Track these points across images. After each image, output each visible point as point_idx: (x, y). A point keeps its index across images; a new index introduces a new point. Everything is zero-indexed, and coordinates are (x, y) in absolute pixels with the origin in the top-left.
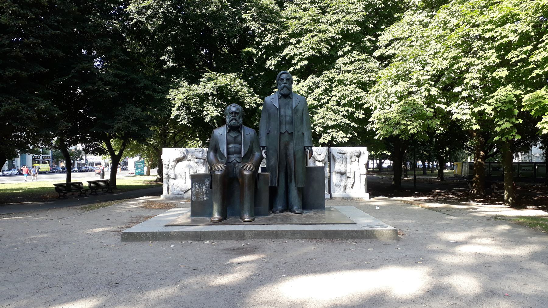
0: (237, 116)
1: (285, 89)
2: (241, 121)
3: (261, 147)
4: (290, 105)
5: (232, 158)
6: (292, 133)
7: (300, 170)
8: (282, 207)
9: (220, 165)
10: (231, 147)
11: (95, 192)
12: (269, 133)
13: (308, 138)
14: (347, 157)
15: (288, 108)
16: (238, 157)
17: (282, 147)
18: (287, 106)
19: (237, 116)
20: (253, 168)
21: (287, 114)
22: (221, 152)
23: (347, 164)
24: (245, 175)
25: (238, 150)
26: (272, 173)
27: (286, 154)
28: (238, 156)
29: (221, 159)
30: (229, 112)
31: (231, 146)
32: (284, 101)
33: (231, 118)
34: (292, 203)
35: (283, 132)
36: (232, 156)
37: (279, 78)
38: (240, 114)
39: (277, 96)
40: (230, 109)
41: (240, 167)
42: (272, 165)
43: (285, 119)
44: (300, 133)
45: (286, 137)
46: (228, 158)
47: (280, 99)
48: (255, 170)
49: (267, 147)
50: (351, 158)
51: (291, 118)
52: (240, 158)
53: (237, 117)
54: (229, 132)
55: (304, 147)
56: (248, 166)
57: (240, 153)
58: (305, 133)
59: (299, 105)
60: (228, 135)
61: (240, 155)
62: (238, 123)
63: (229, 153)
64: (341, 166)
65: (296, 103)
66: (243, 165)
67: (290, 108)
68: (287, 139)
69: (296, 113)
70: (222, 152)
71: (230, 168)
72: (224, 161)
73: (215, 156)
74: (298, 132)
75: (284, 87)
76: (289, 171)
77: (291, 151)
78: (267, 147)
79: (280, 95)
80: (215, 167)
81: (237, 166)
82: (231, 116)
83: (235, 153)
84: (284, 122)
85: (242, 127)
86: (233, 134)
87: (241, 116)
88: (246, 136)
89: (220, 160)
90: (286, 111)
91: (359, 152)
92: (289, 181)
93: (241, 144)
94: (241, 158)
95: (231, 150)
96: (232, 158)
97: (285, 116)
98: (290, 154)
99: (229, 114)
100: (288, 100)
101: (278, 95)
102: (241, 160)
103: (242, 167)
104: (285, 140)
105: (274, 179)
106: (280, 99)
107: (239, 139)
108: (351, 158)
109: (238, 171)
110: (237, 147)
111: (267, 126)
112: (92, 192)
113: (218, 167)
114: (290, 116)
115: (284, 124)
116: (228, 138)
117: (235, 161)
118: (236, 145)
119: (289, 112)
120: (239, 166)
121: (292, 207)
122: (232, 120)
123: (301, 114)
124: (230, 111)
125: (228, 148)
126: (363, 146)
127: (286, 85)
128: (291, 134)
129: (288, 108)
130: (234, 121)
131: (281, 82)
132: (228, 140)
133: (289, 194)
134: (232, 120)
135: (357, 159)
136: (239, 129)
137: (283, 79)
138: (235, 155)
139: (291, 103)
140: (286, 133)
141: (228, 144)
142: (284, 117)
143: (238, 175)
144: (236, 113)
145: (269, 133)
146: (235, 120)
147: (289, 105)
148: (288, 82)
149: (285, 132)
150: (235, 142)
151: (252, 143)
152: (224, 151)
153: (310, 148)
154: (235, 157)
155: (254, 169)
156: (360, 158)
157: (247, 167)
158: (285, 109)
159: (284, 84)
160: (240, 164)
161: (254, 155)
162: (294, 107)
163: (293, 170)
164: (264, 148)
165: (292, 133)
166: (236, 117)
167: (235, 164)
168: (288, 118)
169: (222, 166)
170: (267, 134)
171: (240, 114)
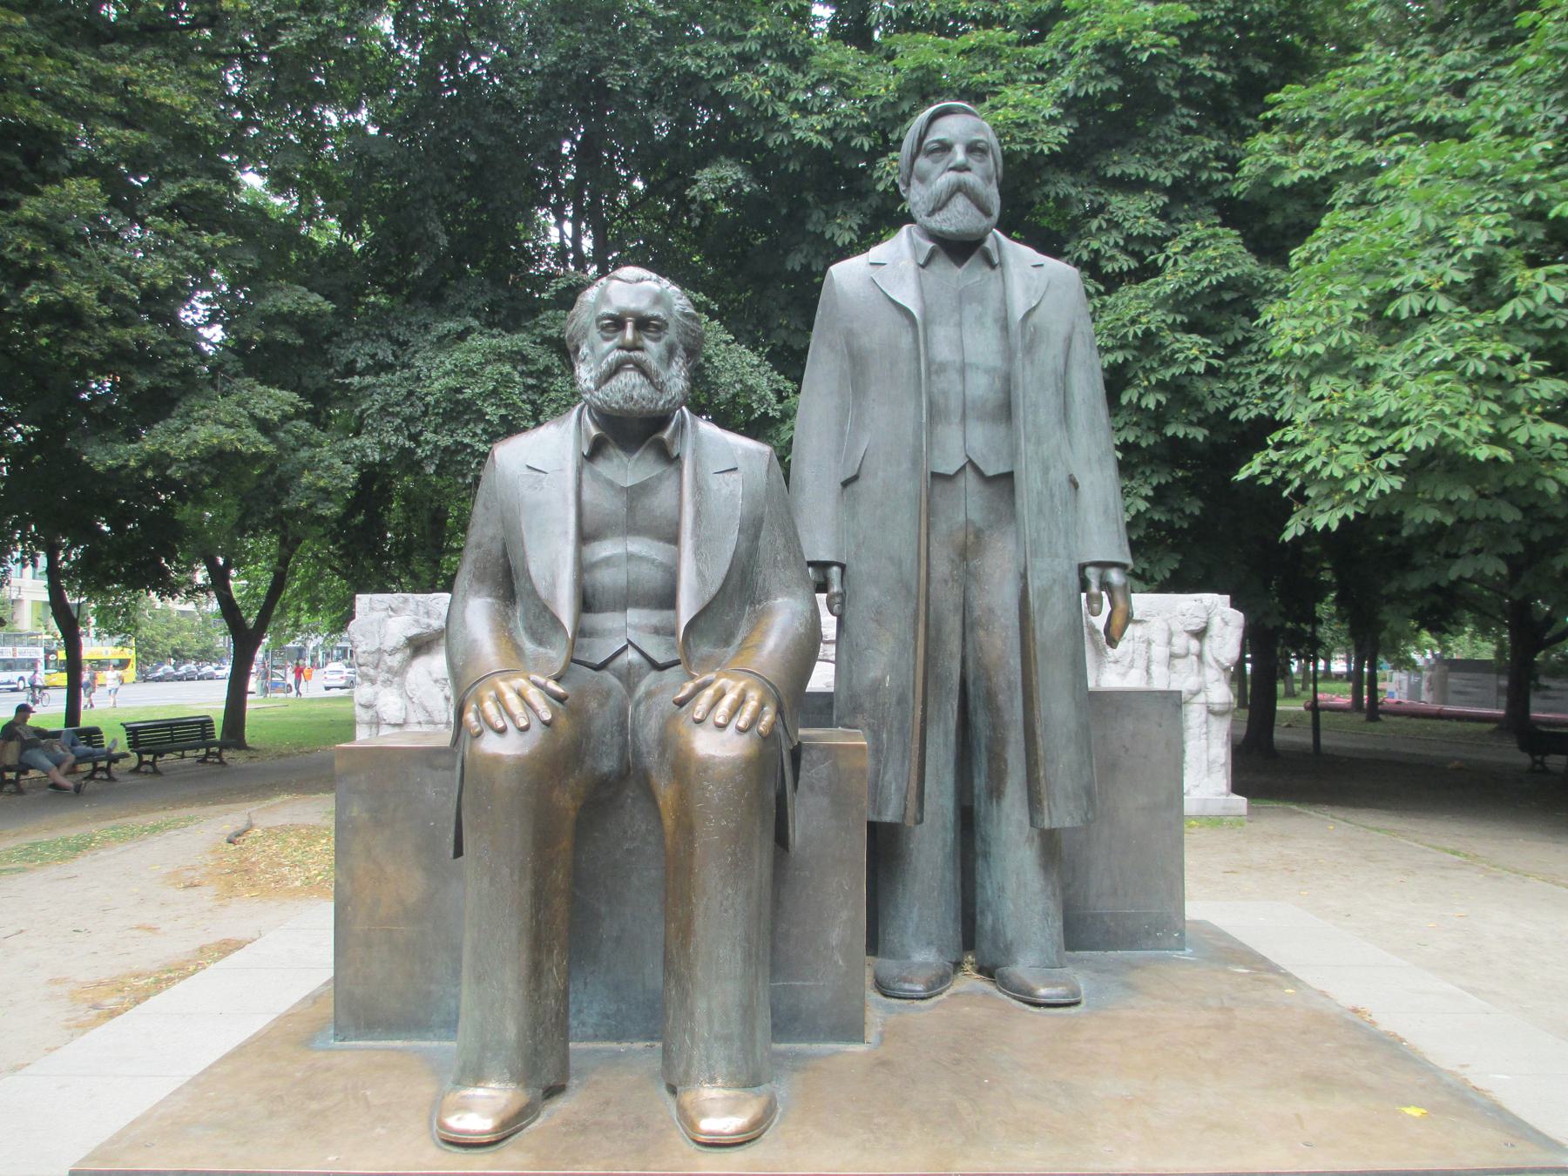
0: (648, 343)
1: (960, 202)
2: (677, 379)
3: (810, 564)
4: (993, 305)
5: (610, 633)
6: (1009, 477)
7: (1057, 710)
8: (941, 952)
9: (520, 682)
10: (607, 561)
11: (153, 763)
12: (855, 478)
13: (1105, 512)
14: (1154, 637)
15: (979, 318)
16: (657, 631)
17: (942, 568)
18: (971, 310)
19: (648, 343)
20: (762, 706)
21: (971, 358)
22: (534, 592)
23: (1153, 668)
24: (705, 765)
25: (651, 577)
26: (875, 735)
27: (965, 608)
28: (655, 617)
29: (539, 640)
30: (599, 320)
31: (605, 549)
32: (949, 274)
33: (610, 358)
34: (1010, 935)
35: (950, 469)
36: (607, 621)
37: (921, 139)
38: (671, 335)
39: (906, 251)
40: (604, 298)
41: (666, 701)
42: (876, 687)
43: (959, 388)
44: (1058, 476)
45: (970, 503)
46: (581, 632)
47: (923, 266)
48: (774, 724)
49: (843, 567)
50: (1169, 643)
51: (998, 384)
52: (667, 631)
53: (653, 350)
54: (596, 450)
55: (1082, 568)
56: (721, 694)
57: (668, 600)
58: (1084, 485)
59: (1043, 305)
60: (586, 476)
61: (670, 613)
62: (659, 387)
63: (587, 602)
64: (1124, 675)
65: (1027, 289)
66: (689, 686)
67: (989, 321)
68: (976, 516)
69: (1030, 349)
70: (542, 588)
71: (593, 705)
72: (557, 655)
73: (503, 626)
74: (1046, 470)
75: (959, 189)
76: (980, 720)
77: (999, 596)
78: (843, 567)
79: (930, 245)
80: (480, 702)
81: (649, 694)
82: (607, 345)
83: (627, 599)
84: (954, 404)
85: (682, 424)
86: (626, 469)
87: (680, 351)
88: (716, 484)
89: (529, 646)
90: (968, 341)
91: (1204, 615)
92: (980, 782)
93: (674, 539)
94: (673, 633)
95: (607, 578)
96: (610, 633)
97: (963, 369)
98: (991, 611)
99: (594, 333)
100: (971, 274)
101: (915, 247)
102: (673, 647)
103: (681, 703)
104: (961, 518)
105: (889, 776)
106: (923, 266)
107: (662, 501)
108: (1169, 643)
109: (650, 731)
110: (653, 561)
111: (842, 434)
112: (141, 763)
113: (499, 699)
114: (995, 369)
115: (956, 419)
116: (587, 495)
117: (632, 656)
118: (638, 546)
119: (983, 346)
120: (662, 689)
121: (1008, 951)
122: (616, 369)
123: (1061, 361)
124: (606, 310)
125: (583, 568)
126: (1221, 593)
127: (967, 177)
128: (1005, 482)
129: (979, 318)
130: (629, 380)
131: (936, 162)
132: (587, 509)
133: (980, 863)
134: (616, 369)
135: (1194, 645)
136: (666, 435)
137: (945, 147)
138: (634, 616)
139: (993, 289)
140: (970, 481)
141: (585, 536)
142: (954, 376)
143: (651, 760)
144: (643, 323)
145: (855, 478)
146: (641, 368)
147: (981, 301)
148: (973, 163)
149: (963, 467)
150: (632, 527)
151: (752, 528)
152: (553, 585)
153: (1115, 576)
154: (636, 627)
155: (768, 718)
156: (1207, 641)
157: (714, 704)
158: (960, 325)
159: (952, 176)
160: (671, 675)
161: (760, 619)
162: (1018, 312)
163: (1014, 712)
164: (822, 566)
165: (1009, 477)
166: (641, 349)
167: (629, 678)
168: (981, 386)
169: (534, 695)
170: (845, 484)
171: (671, 335)
